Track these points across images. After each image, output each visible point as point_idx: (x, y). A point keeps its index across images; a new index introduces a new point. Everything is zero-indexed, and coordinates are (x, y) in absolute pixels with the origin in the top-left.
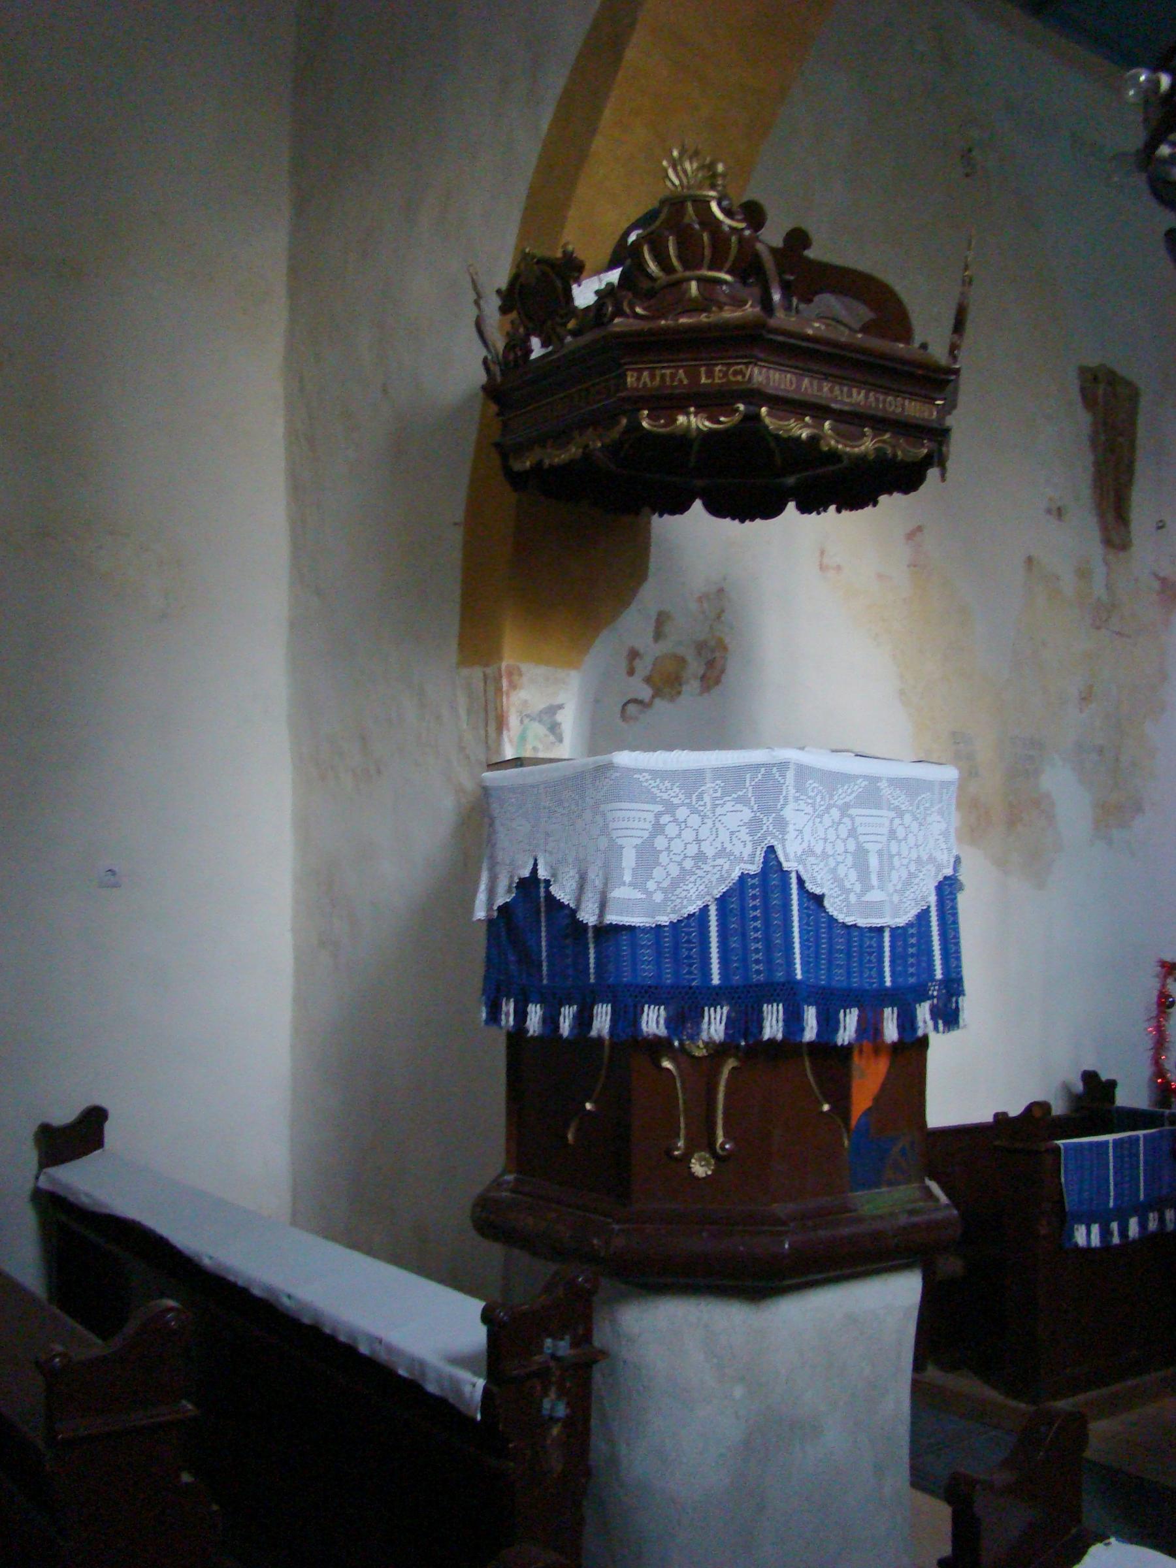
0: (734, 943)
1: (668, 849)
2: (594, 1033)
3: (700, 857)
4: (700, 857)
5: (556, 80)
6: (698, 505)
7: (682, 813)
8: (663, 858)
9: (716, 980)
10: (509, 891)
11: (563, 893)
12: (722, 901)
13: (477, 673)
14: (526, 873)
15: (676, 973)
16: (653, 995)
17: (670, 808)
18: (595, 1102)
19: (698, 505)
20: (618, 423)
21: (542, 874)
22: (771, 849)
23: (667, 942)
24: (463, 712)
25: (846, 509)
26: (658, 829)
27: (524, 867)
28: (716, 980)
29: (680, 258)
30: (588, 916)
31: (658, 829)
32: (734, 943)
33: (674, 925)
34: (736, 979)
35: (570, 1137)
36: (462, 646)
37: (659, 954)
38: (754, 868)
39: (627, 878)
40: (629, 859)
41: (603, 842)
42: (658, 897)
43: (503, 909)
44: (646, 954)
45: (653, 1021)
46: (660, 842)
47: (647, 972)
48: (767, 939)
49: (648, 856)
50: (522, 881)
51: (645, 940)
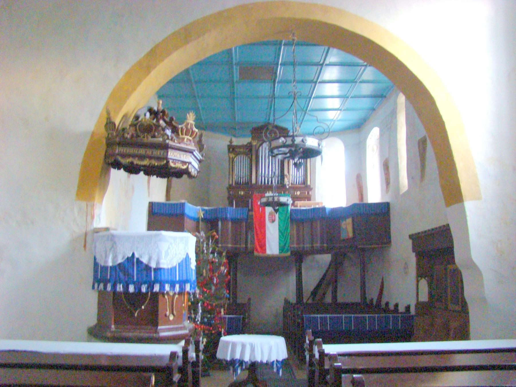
0: (181, 271)
1: (171, 252)
2: (154, 290)
3: (176, 254)
4: (176, 254)
5: (125, 67)
6: (122, 169)
7: (173, 245)
8: (170, 254)
9: (178, 279)
10: (123, 258)
11: (145, 260)
12: (179, 264)
13: (84, 204)
14: (130, 255)
15: (171, 277)
16: (167, 282)
17: (171, 244)
18: (144, 307)
19: (122, 169)
20: (164, 161)
21: (137, 256)
22: (187, 254)
23: (170, 271)
24: (76, 213)
25: (159, 177)
26: (169, 248)
27: (130, 254)
28: (178, 279)
29: (185, 134)
30: (153, 265)
31: (169, 248)
32: (181, 271)
33: (171, 269)
34: (181, 279)
35: (136, 315)
36: (77, 195)
37: (168, 273)
38: (184, 257)
39: (163, 258)
40: (163, 254)
41: (157, 250)
42: (169, 262)
43: (120, 264)
44: (166, 274)
45: (167, 287)
46: (169, 251)
47: (166, 277)
48: (186, 271)
49: (167, 253)
50: (128, 258)
51: (166, 271)
